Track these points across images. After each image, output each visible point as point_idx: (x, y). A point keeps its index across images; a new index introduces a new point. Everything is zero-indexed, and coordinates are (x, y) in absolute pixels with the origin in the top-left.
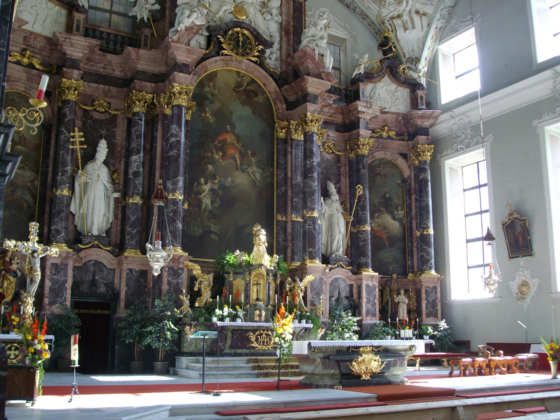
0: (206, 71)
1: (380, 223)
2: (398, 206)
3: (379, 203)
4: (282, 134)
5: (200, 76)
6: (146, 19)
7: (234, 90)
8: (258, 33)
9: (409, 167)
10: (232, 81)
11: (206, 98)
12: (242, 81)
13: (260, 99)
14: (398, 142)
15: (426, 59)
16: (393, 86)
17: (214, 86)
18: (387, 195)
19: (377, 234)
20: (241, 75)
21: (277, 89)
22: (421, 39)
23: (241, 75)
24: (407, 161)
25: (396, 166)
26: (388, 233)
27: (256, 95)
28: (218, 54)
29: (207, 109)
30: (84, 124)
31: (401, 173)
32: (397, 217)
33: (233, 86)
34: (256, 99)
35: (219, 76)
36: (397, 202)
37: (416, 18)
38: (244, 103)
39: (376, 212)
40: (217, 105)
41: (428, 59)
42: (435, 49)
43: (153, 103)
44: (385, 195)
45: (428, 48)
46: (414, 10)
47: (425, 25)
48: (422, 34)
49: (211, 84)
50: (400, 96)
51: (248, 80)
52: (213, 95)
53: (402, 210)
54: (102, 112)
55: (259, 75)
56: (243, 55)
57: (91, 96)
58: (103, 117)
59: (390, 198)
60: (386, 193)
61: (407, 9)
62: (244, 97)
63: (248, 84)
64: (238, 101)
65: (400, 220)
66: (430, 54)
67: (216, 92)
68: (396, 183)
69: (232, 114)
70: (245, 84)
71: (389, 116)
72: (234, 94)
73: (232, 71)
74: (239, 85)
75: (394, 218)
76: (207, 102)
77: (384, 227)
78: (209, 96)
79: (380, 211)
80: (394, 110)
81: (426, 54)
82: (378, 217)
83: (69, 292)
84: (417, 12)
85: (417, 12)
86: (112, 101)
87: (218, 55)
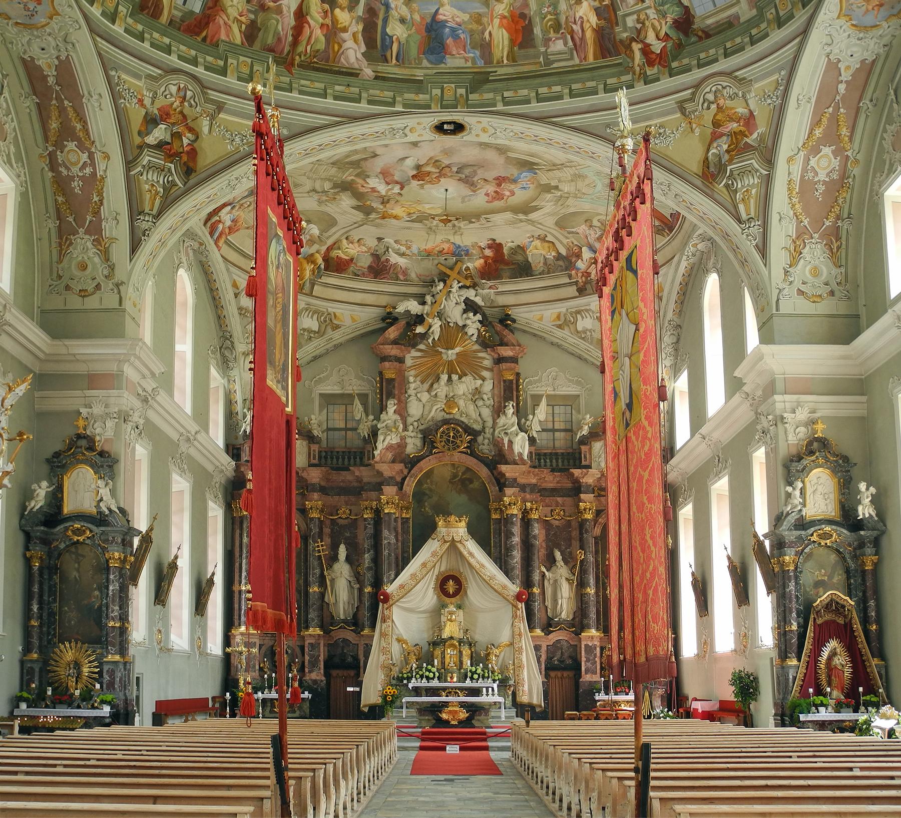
8: (466, 425)
43: (377, 508)
83: (322, 663)
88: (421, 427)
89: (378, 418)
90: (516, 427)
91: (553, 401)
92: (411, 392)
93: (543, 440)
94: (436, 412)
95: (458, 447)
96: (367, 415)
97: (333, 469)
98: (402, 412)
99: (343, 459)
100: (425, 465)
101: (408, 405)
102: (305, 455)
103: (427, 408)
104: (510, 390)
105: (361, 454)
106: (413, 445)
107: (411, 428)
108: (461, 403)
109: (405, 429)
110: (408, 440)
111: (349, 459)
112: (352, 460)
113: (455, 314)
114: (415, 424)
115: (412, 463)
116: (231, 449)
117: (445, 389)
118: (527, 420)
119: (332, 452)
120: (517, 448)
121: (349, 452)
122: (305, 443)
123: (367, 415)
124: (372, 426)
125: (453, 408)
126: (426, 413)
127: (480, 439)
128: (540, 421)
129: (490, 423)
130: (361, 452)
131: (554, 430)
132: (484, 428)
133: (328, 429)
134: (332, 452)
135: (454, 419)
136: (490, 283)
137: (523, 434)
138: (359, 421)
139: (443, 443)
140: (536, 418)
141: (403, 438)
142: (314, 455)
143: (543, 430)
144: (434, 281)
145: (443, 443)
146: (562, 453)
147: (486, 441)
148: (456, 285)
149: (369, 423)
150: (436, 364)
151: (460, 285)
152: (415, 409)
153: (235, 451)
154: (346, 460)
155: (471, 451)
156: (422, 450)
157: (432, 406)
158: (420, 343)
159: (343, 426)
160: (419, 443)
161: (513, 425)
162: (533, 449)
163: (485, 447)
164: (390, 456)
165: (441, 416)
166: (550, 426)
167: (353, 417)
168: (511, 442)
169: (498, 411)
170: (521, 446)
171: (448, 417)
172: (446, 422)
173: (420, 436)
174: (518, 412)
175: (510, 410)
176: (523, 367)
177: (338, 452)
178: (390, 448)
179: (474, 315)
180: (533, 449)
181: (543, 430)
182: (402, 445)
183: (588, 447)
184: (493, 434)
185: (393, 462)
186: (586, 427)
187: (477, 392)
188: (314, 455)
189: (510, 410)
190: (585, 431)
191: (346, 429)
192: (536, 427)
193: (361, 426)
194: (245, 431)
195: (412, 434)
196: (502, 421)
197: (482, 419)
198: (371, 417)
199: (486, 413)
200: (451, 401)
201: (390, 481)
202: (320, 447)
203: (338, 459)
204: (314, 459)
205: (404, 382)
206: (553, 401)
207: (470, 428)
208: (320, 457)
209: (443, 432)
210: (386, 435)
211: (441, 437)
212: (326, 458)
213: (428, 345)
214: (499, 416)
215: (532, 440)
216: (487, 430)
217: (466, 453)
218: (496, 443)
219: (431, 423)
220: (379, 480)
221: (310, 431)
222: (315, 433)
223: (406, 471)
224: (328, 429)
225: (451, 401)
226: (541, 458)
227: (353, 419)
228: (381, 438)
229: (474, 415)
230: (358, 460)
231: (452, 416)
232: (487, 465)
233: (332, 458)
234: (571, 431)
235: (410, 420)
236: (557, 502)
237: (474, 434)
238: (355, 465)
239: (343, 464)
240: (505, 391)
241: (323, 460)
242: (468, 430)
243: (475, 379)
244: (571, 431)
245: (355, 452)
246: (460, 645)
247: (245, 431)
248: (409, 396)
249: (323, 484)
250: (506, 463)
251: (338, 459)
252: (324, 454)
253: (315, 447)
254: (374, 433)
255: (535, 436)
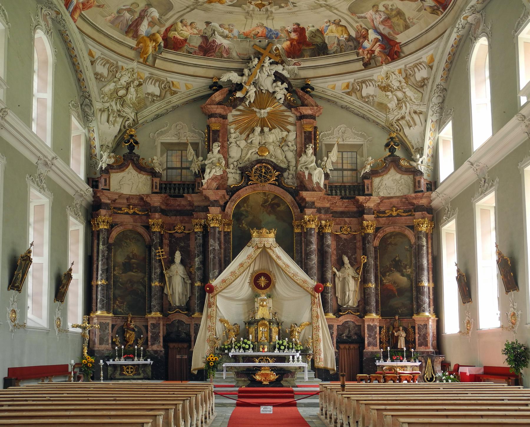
0: (239, 198)
1: (391, 279)
2: (406, 265)
3: (390, 265)
4: (297, 230)
5: (236, 201)
6: (197, 172)
7: (262, 205)
8: (275, 164)
9: (415, 236)
10: (260, 199)
11: (242, 214)
12: (268, 199)
13: (282, 208)
14: (406, 217)
15: (429, 147)
16: (398, 176)
17: (247, 206)
18: (397, 259)
19: (388, 288)
20: (267, 194)
21: (293, 199)
22: (422, 132)
23: (267, 194)
24: (413, 231)
25: (405, 236)
26: (398, 286)
27: (278, 205)
28: (247, 185)
29: (243, 222)
30: (170, 241)
31: (409, 240)
32: (405, 274)
33: (261, 203)
34: (279, 209)
35: (250, 199)
36: (406, 263)
37: (416, 117)
38: (269, 213)
39: (388, 272)
40: (250, 218)
41: (431, 147)
42: (436, 138)
44: (395, 259)
45: (428, 138)
46: (412, 111)
47: (423, 122)
48: (423, 128)
49: (245, 205)
50: (403, 183)
51: (272, 196)
52: (247, 211)
53: (410, 268)
54: (181, 233)
55: (279, 191)
56: (266, 181)
57: (173, 224)
58: (181, 235)
59: (400, 261)
60: (397, 257)
61: (408, 111)
62: (269, 209)
63: (272, 200)
64: (265, 213)
65: (408, 276)
66: (432, 143)
67: (249, 209)
68: (405, 248)
69: (261, 222)
70: (270, 200)
71: (394, 200)
72: (262, 208)
73: (260, 193)
74: (266, 201)
75: (403, 275)
76: (243, 217)
77: (394, 282)
78: (244, 213)
79: (391, 271)
80: (398, 194)
81: (428, 143)
82: (389, 276)
84: (415, 112)
85: (415, 112)
86: (186, 225)
87: (248, 185)
88: (240, 166)
89: (205, 158)
90: (314, 164)
91: (342, 149)
92: (232, 140)
93: (335, 177)
94: (251, 155)
95: (269, 180)
96: (198, 157)
97: (171, 196)
98: (225, 151)
99: (179, 190)
100: (243, 193)
101: (230, 150)
102: (149, 187)
103: (244, 152)
104: (309, 138)
105: (193, 185)
106: (233, 178)
107: (232, 166)
108: (271, 148)
109: (227, 165)
110: (230, 175)
111: (184, 190)
112: (186, 190)
113: (267, 82)
114: (235, 163)
115: (232, 191)
116: (91, 181)
117: (259, 138)
118: (322, 161)
119: (170, 184)
120: (315, 179)
121: (184, 184)
122: (149, 177)
123: (198, 157)
124: (202, 165)
125: (264, 152)
126: (243, 155)
127: (285, 174)
128: (333, 163)
129: (293, 163)
130: (193, 185)
131: (343, 170)
132: (289, 166)
133: (168, 168)
134: (170, 184)
135: (265, 160)
136: (294, 61)
137: (320, 169)
138: (191, 162)
139: (257, 177)
140: (329, 159)
141: (224, 172)
142: (156, 186)
143: (335, 170)
144: (250, 59)
145: (257, 177)
146: (350, 186)
147: (291, 176)
148: (267, 61)
149: (199, 163)
150: (251, 120)
151: (271, 61)
152: (235, 153)
153: (94, 183)
154: (181, 190)
155: (279, 183)
156: (240, 183)
157: (248, 150)
158: (240, 105)
159: (179, 165)
160: (238, 177)
161: (312, 162)
162: (327, 182)
163: (289, 180)
164: (214, 185)
165: (255, 157)
166: (340, 166)
167: (187, 159)
168: (310, 175)
169: (300, 153)
170: (318, 177)
171: (261, 158)
172: (258, 161)
173: (239, 172)
174: (315, 153)
175: (310, 151)
176: (318, 123)
177: (175, 184)
178: (215, 178)
179: (282, 84)
180: (327, 182)
181: (335, 170)
182: (224, 178)
183: (370, 181)
184: (296, 171)
185: (218, 189)
186: (369, 167)
187: (284, 140)
188: (156, 186)
189: (310, 151)
190: (368, 169)
191: (182, 168)
192: (329, 166)
193: (193, 165)
194: (101, 168)
195: (233, 171)
196: (303, 159)
197: (287, 160)
198: (201, 158)
199: (291, 156)
200: (263, 147)
201: (215, 203)
202: (161, 180)
203: (175, 189)
204: (156, 188)
205: (227, 133)
206: (342, 149)
207: (278, 166)
208: (161, 188)
209: (257, 169)
210: (211, 169)
211: (255, 172)
212: (165, 188)
213: (245, 107)
214: (300, 156)
215: (327, 176)
216: (291, 168)
217: (275, 185)
218: (299, 177)
219: (248, 162)
220: (206, 204)
221: (153, 169)
222: (157, 170)
223: (227, 197)
224: (168, 168)
225: (263, 147)
226: (332, 189)
227: (187, 161)
228: (207, 171)
229: (281, 157)
230: (191, 190)
231: (263, 158)
232: (291, 193)
233: (170, 189)
234: (356, 170)
235: (231, 161)
236: (345, 221)
237: (282, 170)
238: (188, 193)
239: (179, 193)
240: (305, 139)
241: (163, 191)
242: (276, 167)
243: (282, 131)
244: (356, 170)
245: (188, 185)
246: (270, 324)
247: (101, 168)
248: (231, 143)
249: (163, 207)
250: (307, 190)
251: (175, 189)
252: (164, 186)
253: (157, 180)
254: (203, 170)
255: (329, 172)
